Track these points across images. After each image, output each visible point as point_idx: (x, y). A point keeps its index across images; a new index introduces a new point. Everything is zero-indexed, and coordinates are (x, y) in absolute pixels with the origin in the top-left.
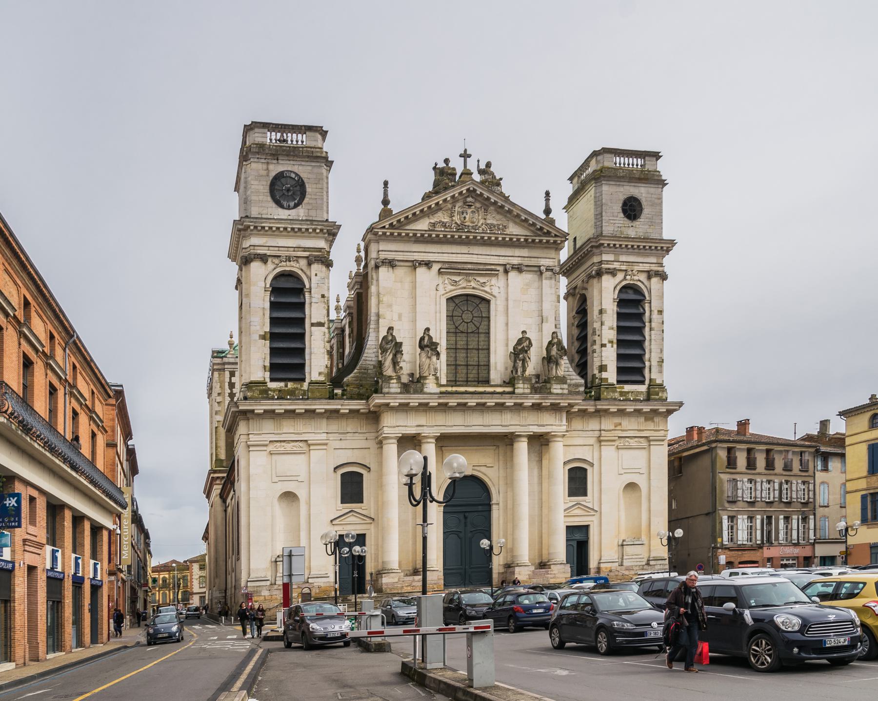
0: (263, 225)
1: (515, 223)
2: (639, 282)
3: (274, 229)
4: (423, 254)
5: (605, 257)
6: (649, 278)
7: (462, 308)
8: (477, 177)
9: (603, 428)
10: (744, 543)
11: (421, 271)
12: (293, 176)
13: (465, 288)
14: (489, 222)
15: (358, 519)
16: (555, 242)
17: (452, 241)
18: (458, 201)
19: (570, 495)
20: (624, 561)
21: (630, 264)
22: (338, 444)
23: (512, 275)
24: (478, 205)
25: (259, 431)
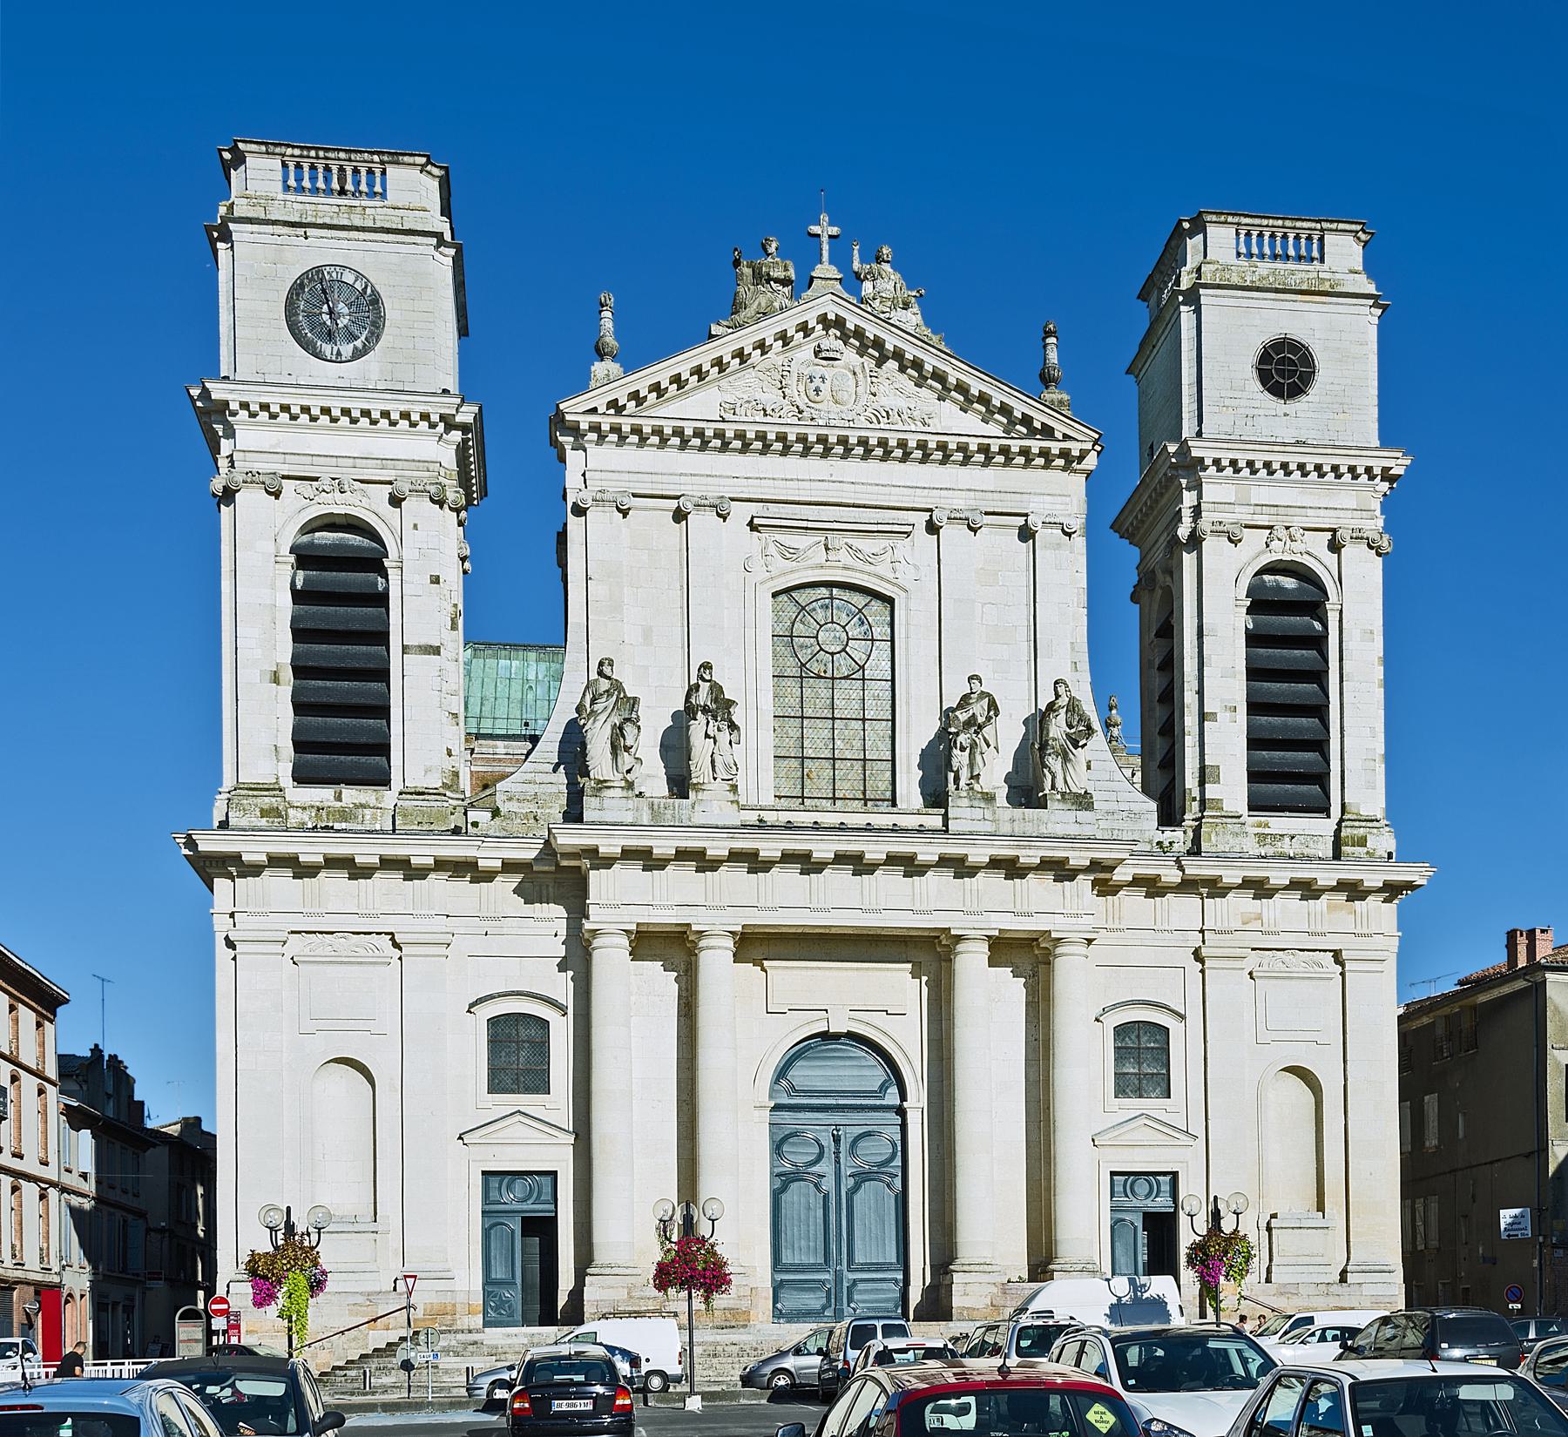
2: (1305, 556)
6: (1335, 547)
16: (1065, 454)
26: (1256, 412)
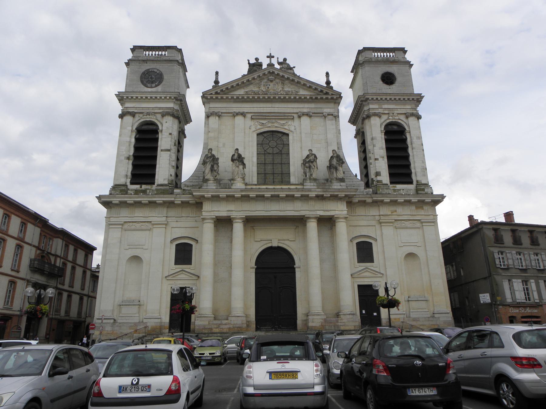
0: (132, 96)
1: (303, 89)
3: (139, 98)
4: (239, 109)
5: (371, 106)
6: (407, 117)
7: (269, 139)
8: (277, 66)
9: (381, 213)
10: (523, 301)
11: (239, 119)
12: (156, 71)
13: (269, 127)
14: (285, 89)
15: (187, 276)
16: (332, 98)
17: (259, 100)
18: (263, 79)
19: (358, 262)
20: (411, 313)
21: (391, 110)
22: (174, 224)
23: (305, 120)
24: (277, 81)
25: (117, 215)
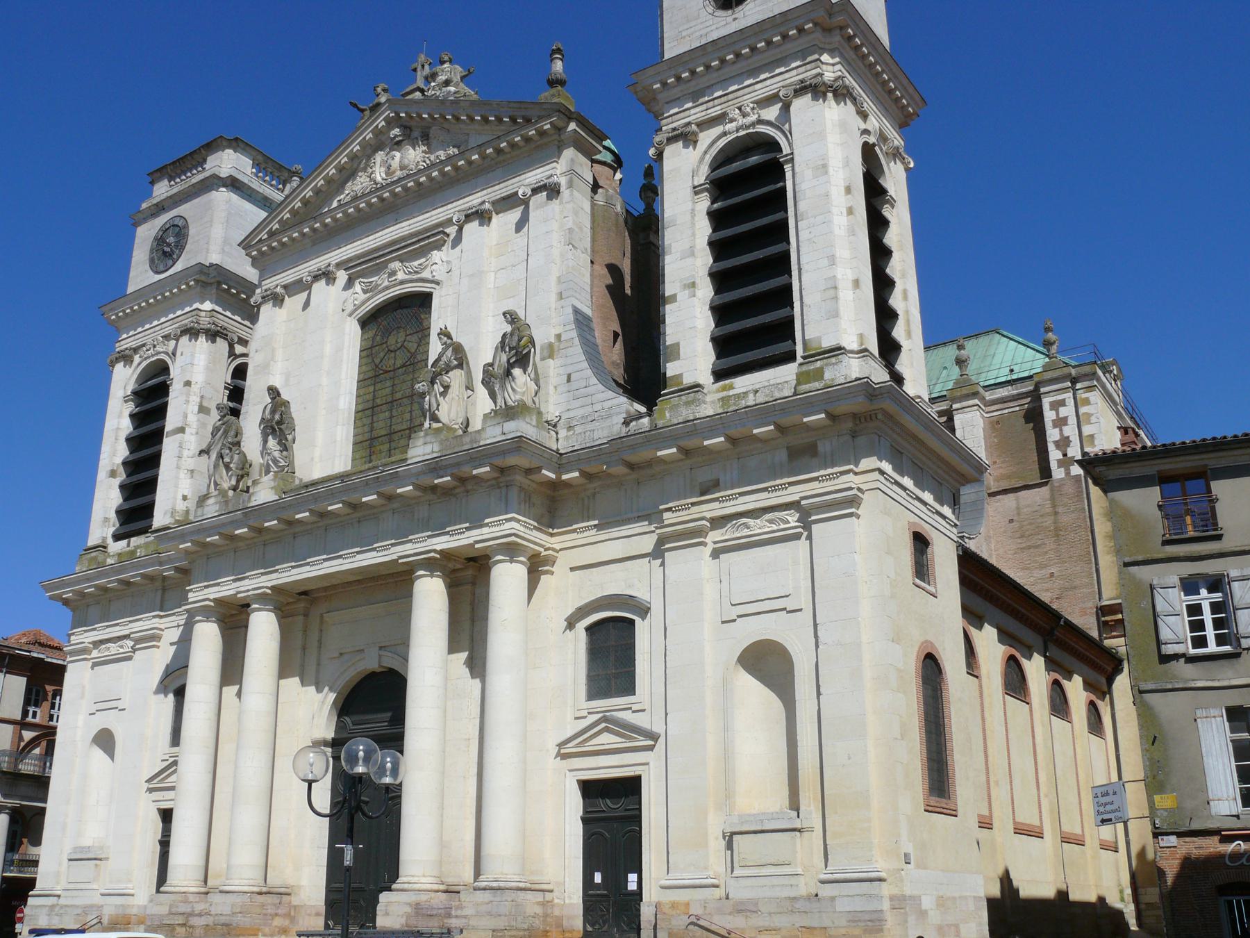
26: (709, 29)
